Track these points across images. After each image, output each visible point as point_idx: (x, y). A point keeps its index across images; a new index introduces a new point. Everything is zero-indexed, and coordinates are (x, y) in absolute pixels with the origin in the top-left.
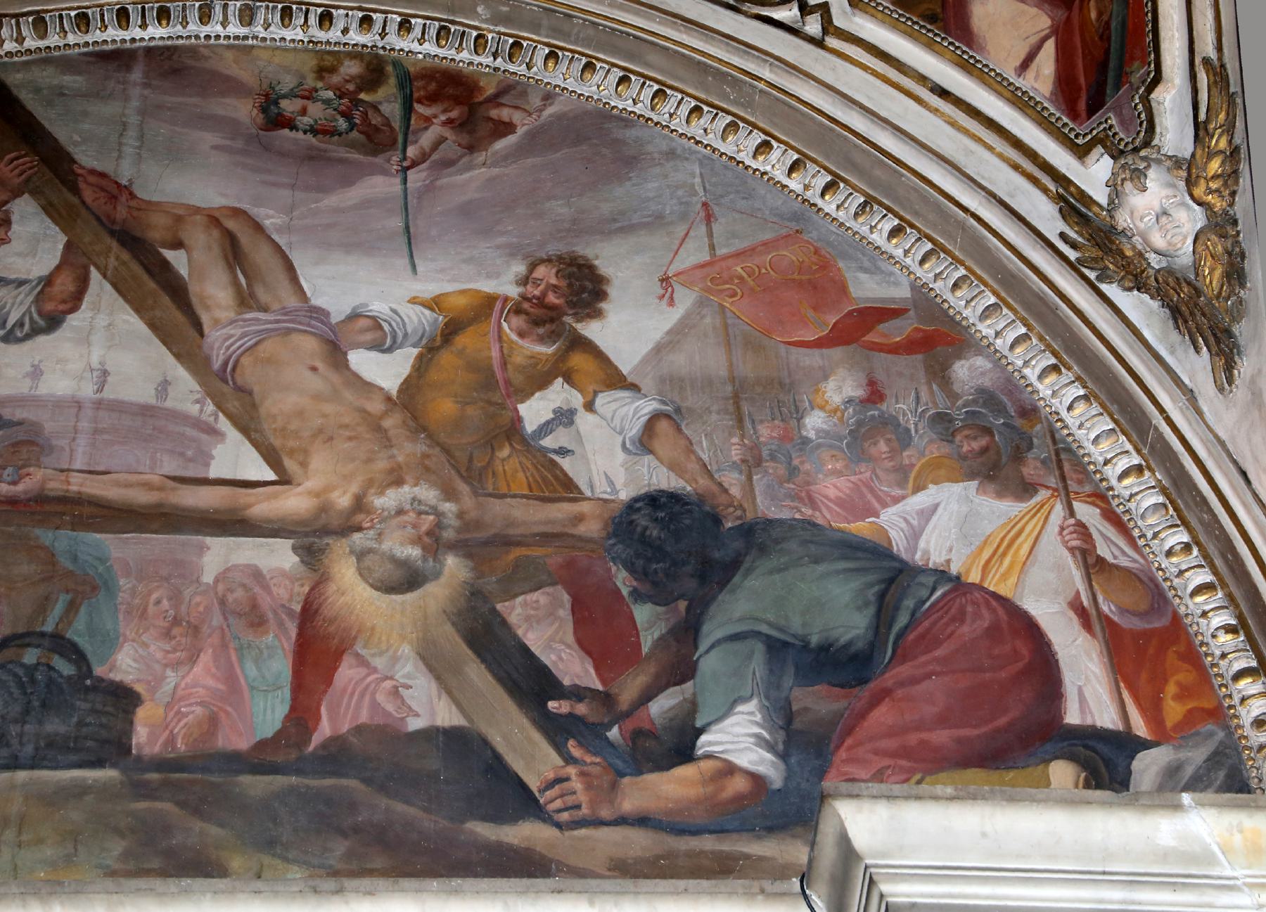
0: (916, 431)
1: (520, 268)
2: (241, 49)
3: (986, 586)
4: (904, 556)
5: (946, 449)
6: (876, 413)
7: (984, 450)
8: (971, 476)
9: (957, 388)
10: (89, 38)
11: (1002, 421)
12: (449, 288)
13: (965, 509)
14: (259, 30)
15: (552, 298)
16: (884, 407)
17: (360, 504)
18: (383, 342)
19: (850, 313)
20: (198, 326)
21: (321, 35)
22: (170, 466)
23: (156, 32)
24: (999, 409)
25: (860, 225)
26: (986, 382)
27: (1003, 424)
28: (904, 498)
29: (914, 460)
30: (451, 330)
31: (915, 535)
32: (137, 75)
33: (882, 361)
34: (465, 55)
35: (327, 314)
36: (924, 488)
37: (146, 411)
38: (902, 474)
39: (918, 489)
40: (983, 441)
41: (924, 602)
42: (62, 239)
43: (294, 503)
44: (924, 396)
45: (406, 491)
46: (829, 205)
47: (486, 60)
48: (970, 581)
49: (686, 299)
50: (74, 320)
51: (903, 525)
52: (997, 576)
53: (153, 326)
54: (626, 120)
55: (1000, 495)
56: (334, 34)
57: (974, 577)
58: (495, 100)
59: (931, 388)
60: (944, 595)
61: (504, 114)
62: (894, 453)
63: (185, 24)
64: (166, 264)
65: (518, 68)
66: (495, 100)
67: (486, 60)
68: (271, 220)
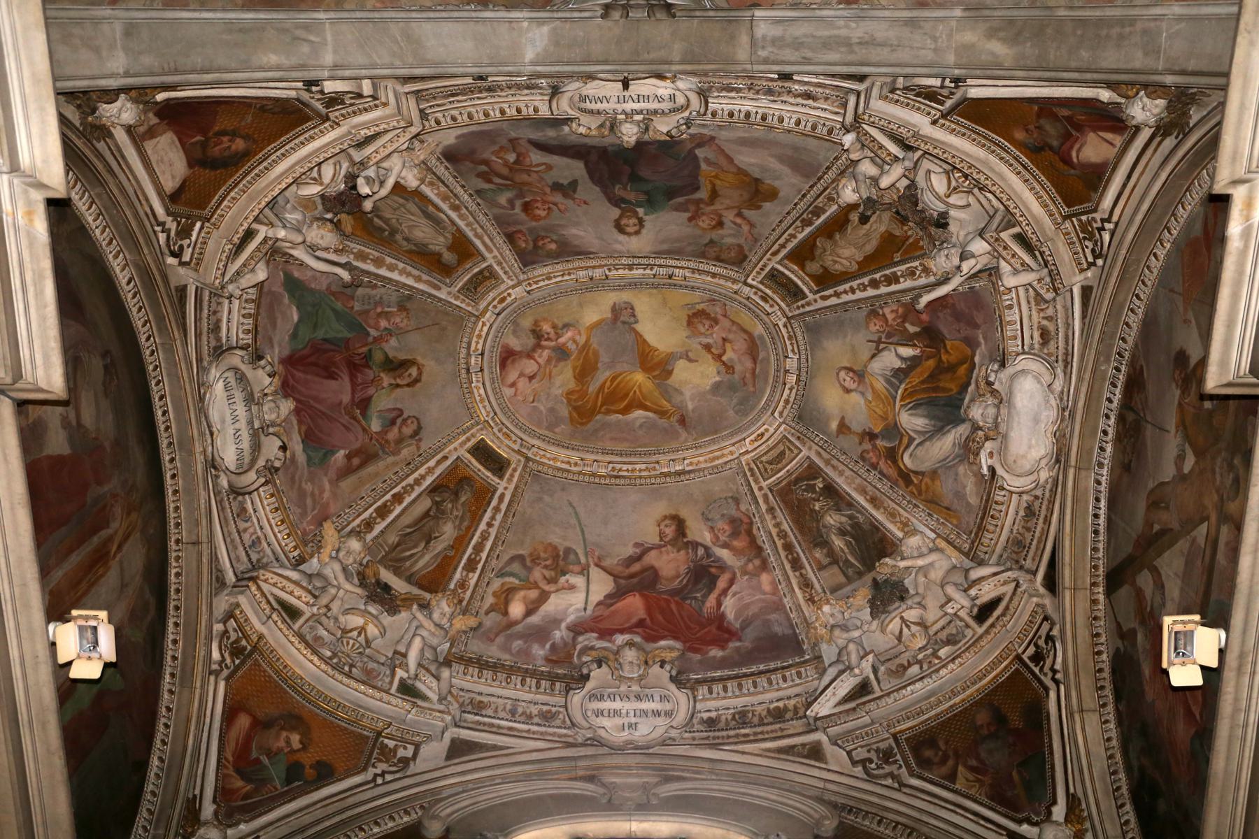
1: (1174, 386)
2: (1112, 470)
10: (1102, 531)
12: (1174, 421)
14: (1106, 462)
15: (1183, 375)
17: (1217, 491)
18: (1181, 458)
20: (1172, 529)
21: (1110, 436)
22: (1199, 562)
23: (1103, 504)
25: (1182, 221)
30: (1185, 428)
32: (1113, 517)
34: (1121, 377)
35: (1174, 477)
37: (1187, 563)
42: (1146, 570)
43: (1213, 518)
45: (1217, 469)
46: (1175, 232)
47: (1123, 368)
49: (1191, 316)
50: (1163, 578)
53: (1169, 548)
54: (1146, 314)
56: (1110, 431)
58: (1135, 369)
61: (1138, 368)
63: (1100, 492)
64: (1156, 533)
65: (1127, 355)
66: (1135, 369)
67: (1123, 369)
68: (1151, 485)
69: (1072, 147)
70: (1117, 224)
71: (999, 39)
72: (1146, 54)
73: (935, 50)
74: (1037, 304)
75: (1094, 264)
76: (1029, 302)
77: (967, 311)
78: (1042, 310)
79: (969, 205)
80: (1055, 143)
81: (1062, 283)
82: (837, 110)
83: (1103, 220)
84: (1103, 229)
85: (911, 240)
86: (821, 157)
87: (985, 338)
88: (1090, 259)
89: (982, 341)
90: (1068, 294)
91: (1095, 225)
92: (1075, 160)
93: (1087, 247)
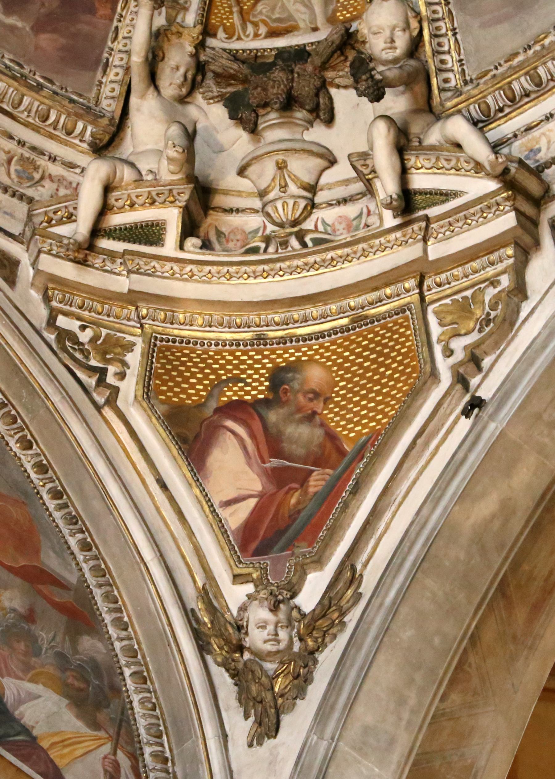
0: (46, 653)
3: (49, 753)
4: (9, 705)
5: (58, 674)
6: (27, 627)
7: (82, 690)
8: (67, 696)
9: (80, 648)
11: (97, 683)
13: (55, 709)
16: (33, 627)
19: (35, 566)
24: (99, 677)
26: (99, 658)
27: (98, 685)
28: (21, 679)
29: (36, 666)
31: (20, 702)
33: (41, 605)
36: (36, 683)
38: (27, 668)
39: (31, 680)
40: (82, 686)
41: (10, 736)
44: (59, 638)
48: (41, 744)
51: (15, 692)
52: (58, 753)
55: (78, 717)
57: (45, 744)
59: (64, 639)
60: (23, 741)
62: (26, 654)
69: (253, 436)
70: (98, 408)
71: (493, 516)
72: (366, 730)
73: (538, 417)
74: (22, 158)
75: (51, 322)
76: (33, 149)
77: (72, 29)
78: (9, 162)
79: (242, 172)
80: (273, 416)
81: (49, 253)
82: (535, 133)
83: (116, 390)
84: (101, 382)
85: (236, 19)
86: (476, 24)
87: (12, 29)
88: (62, 321)
89: (11, 20)
90: (16, 230)
91: (112, 369)
92: (230, 423)
93: (83, 328)
